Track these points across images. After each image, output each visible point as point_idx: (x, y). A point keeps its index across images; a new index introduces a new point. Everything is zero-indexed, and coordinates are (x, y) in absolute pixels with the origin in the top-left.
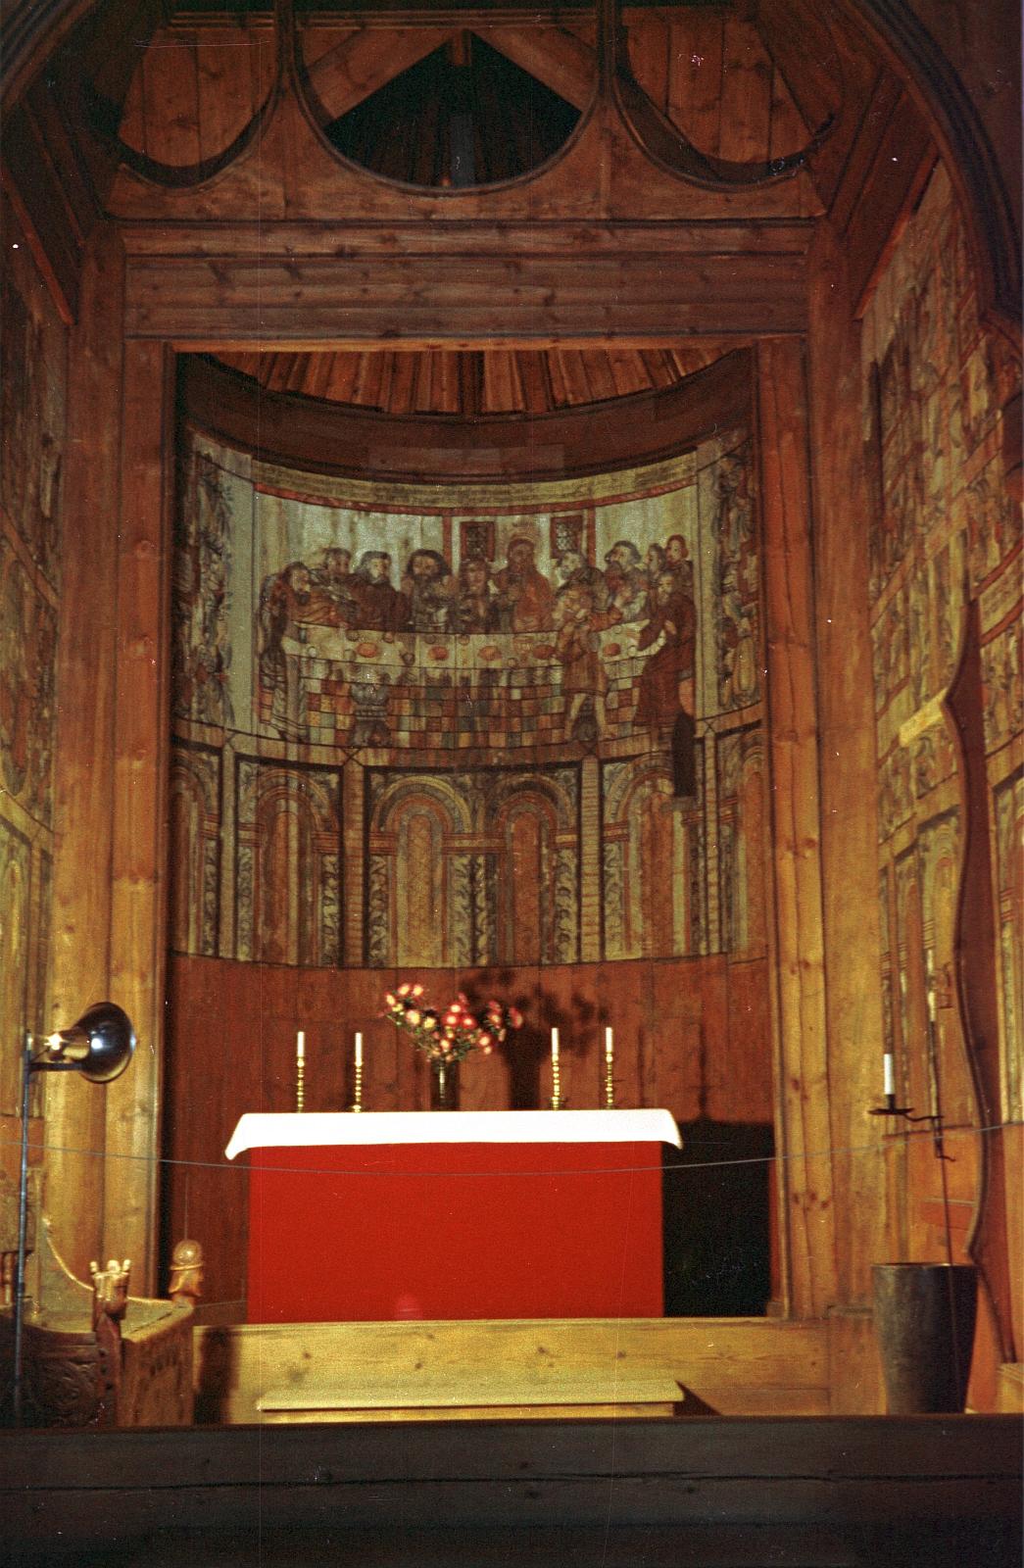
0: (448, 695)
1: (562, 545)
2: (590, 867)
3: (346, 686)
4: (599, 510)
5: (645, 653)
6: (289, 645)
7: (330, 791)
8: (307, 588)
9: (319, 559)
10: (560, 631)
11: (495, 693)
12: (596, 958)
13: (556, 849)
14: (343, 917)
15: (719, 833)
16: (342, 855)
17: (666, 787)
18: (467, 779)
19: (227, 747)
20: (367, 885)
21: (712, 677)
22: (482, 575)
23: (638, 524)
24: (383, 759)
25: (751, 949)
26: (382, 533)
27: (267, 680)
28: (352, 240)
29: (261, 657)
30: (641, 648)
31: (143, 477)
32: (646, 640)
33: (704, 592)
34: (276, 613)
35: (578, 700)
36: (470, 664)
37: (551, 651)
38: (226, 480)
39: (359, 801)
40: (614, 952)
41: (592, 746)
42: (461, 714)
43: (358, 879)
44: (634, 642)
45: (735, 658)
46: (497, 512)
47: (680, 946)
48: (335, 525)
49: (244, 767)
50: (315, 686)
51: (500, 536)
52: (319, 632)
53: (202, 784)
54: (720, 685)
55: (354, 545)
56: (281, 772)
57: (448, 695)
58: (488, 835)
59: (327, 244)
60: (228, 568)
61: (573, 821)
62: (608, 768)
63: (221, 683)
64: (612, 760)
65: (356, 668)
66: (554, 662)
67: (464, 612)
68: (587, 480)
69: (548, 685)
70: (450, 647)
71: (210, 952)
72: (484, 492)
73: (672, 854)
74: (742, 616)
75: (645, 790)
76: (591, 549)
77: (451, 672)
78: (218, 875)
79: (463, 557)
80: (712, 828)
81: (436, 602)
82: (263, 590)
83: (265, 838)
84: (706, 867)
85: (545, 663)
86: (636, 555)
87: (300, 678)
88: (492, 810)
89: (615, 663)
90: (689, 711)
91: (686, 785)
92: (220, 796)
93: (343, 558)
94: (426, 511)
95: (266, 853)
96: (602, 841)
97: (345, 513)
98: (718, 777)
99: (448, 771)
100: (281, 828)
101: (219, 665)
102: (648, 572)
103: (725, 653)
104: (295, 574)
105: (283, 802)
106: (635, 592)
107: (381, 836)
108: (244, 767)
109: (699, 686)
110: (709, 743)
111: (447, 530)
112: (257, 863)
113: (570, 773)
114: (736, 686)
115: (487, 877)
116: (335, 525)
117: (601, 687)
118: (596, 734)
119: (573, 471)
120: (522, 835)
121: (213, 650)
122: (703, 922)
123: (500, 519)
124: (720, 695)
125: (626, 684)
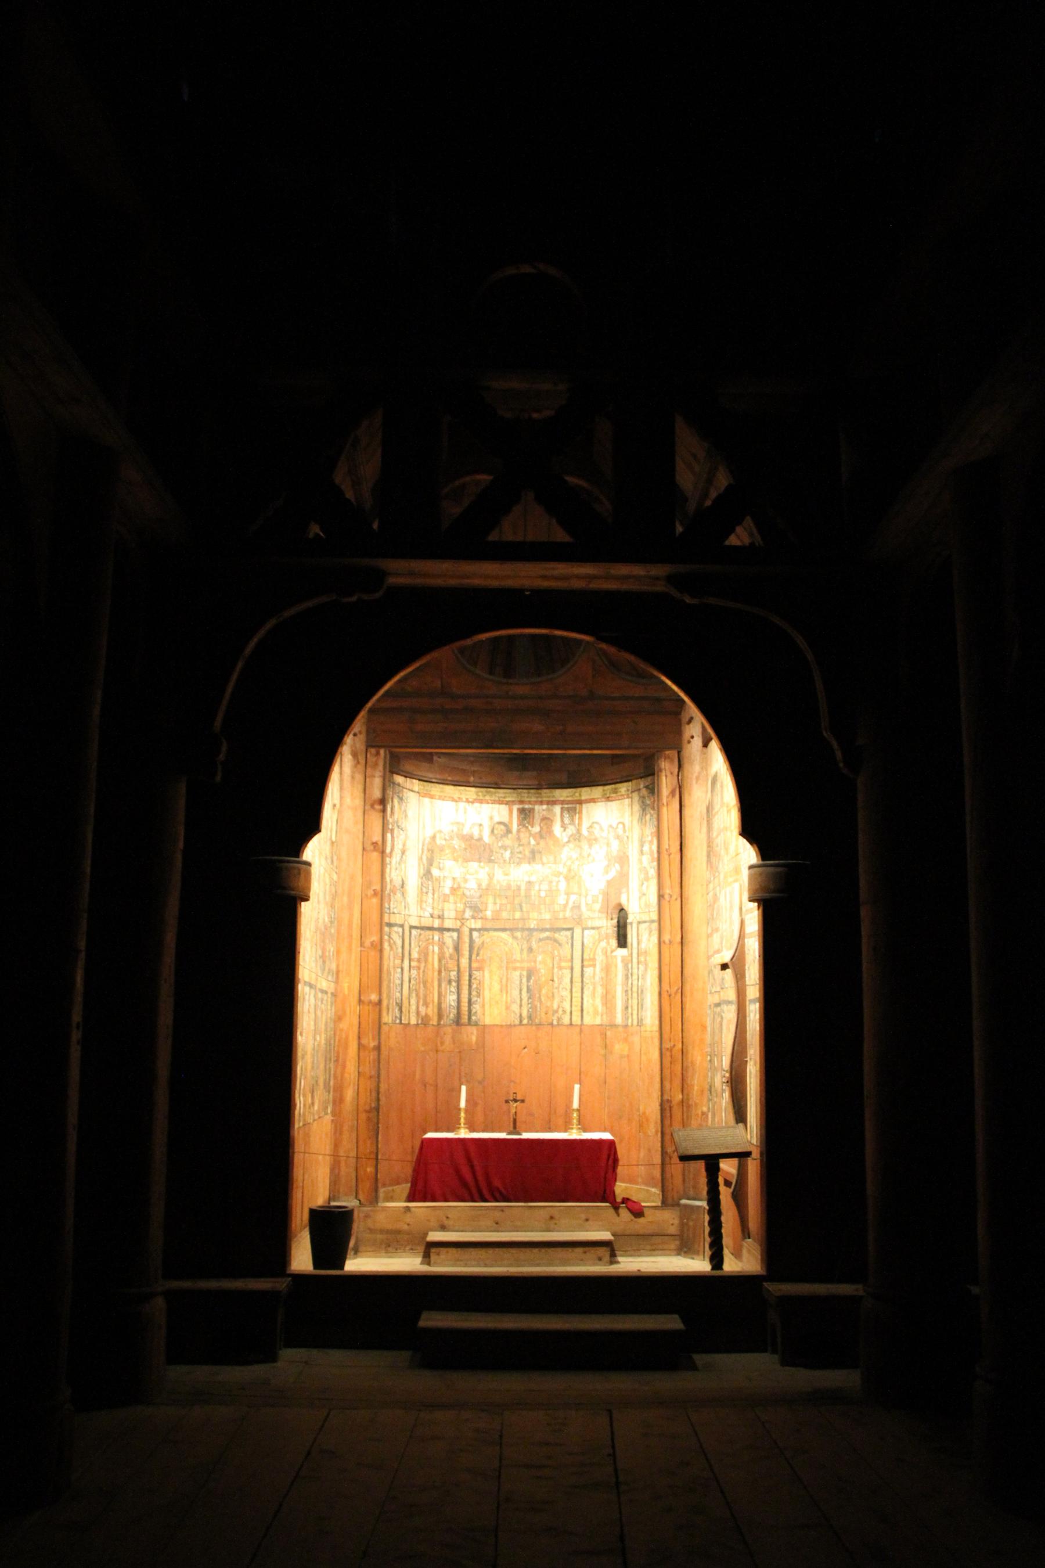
1: (567, 820)
4: (584, 806)
6: (435, 872)
8: (444, 842)
10: (565, 864)
11: (533, 893)
12: (579, 1023)
13: (560, 968)
14: (459, 1001)
16: (459, 971)
17: (614, 942)
18: (518, 934)
20: (470, 986)
22: (527, 835)
24: (478, 924)
25: (653, 1025)
27: (424, 890)
34: (429, 855)
35: (573, 898)
37: (559, 874)
40: (588, 1020)
41: (579, 921)
42: (516, 902)
46: (536, 803)
50: (447, 891)
54: (640, 898)
56: (430, 933)
57: (510, 893)
60: (406, 837)
61: (569, 957)
62: (586, 932)
64: (587, 928)
65: (466, 881)
66: (561, 878)
68: (579, 790)
69: (558, 890)
75: (603, 944)
76: (580, 824)
83: (423, 965)
85: (556, 879)
86: (601, 829)
88: (530, 950)
91: (622, 941)
92: (403, 947)
94: (501, 803)
96: (583, 966)
97: (462, 805)
99: (511, 930)
100: (430, 959)
104: (438, 836)
107: (477, 961)
108: (414, 932)
110: (635, 925)
113: (569, 933)
115: (528, 980)
123: (537, 807)
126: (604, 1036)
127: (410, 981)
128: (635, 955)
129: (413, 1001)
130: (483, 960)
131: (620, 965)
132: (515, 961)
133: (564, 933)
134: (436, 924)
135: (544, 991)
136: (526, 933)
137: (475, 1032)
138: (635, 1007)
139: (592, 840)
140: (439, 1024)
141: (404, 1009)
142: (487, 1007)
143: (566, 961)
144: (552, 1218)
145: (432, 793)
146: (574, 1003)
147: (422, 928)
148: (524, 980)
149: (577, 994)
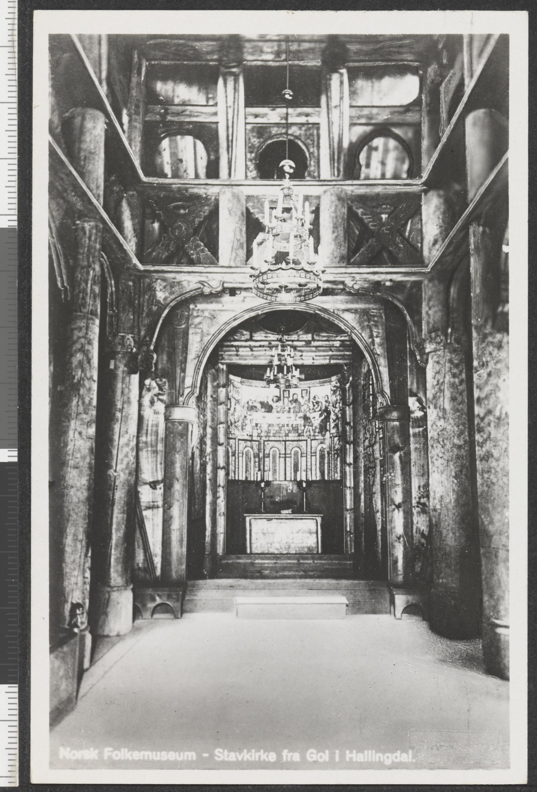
28: (262, 343)
32: (321, 415)
35: (307, 427)
50: (254, 425)
59: (258, 344)
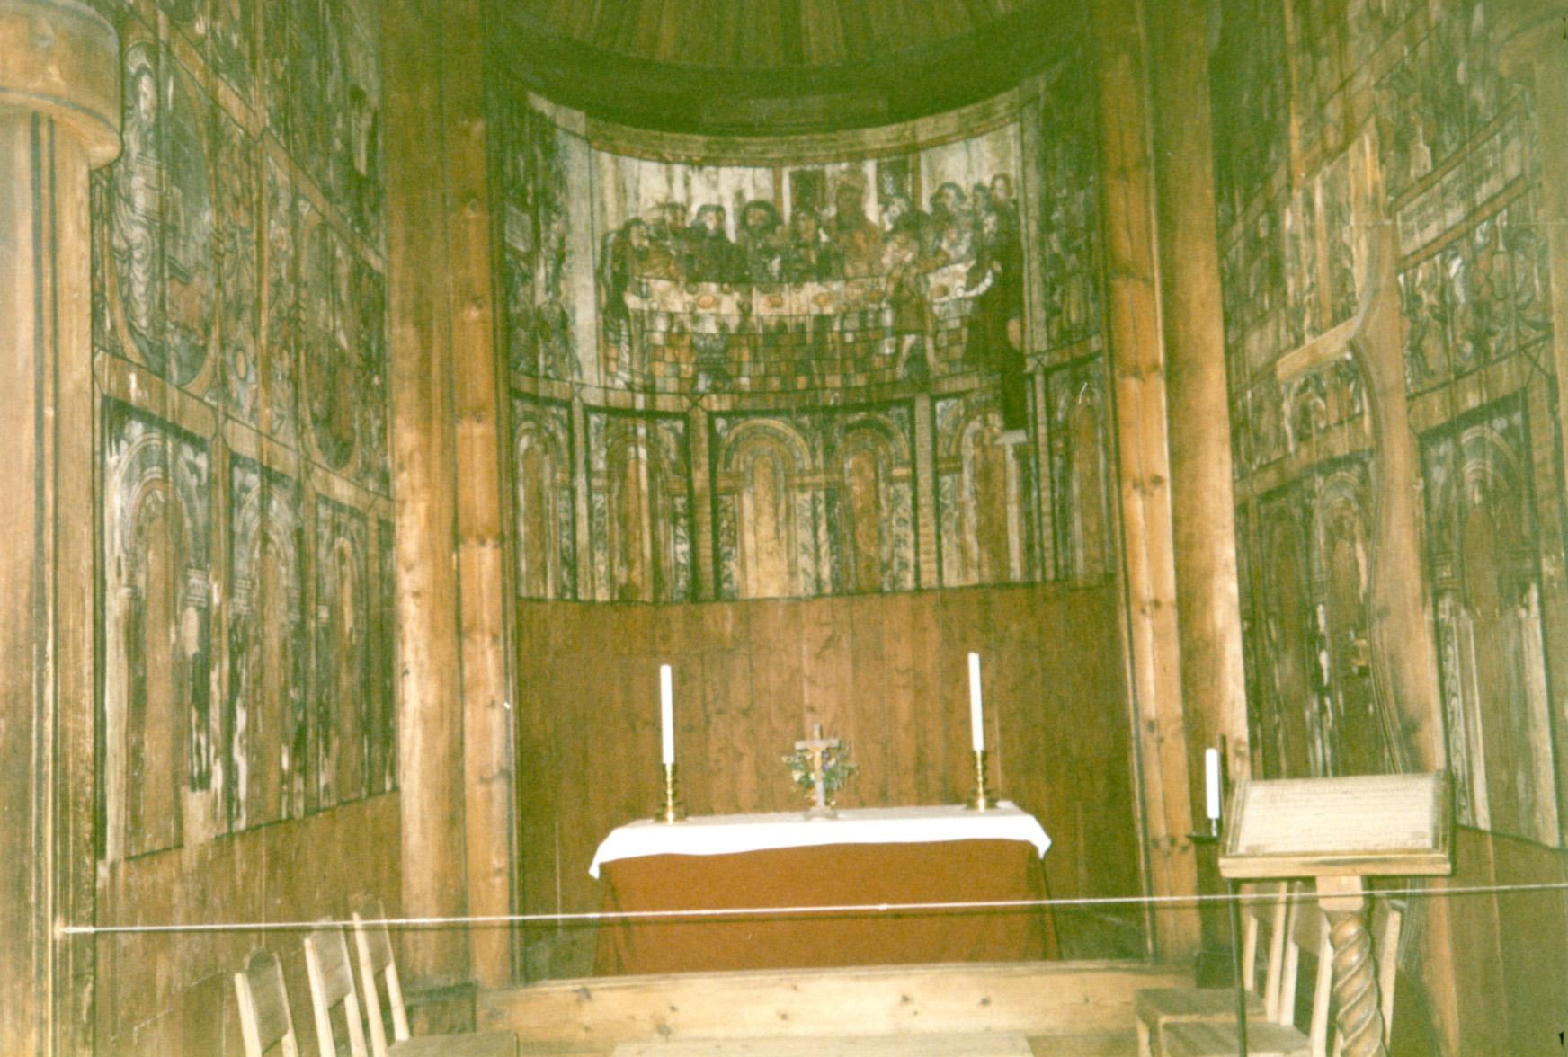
0: (784, 340)
1: (889, 190)
2: (926, 500)
3: (687, 338)
4: (923, 156)
5: (973, 293)
6: (632, 301)
7: (677, 435)
8: (646, 243)
9: (656, 214)
12: (934, 583)
13: (891, 481)
14: (694, 552)
15: (1051, 465)
17: (996, 421)
18: (805, 420)
19: (576, 400)
21: (1040, 315)
22: (812, 223)
23: (963, 165)
24: (726, 405)
26: (715, 185)
27: (611, 336)
29: (605, 312)
30: (967, 289)
31: (467, 132)
32: (973, 278)
33: (1029, 228)
34: (617, 269)
35: (909, 340)
36: (805, 309)
38: (561, 139)
39: (705, 445)
40: (952, 579)
43: (710, 518)
44: (961, 282)
45: (1062, 295)
47: (1016, 570)
48: (670, 180)
49: (594, 419)
50: (658, 338)
51: (830, 186)
52: (661, 285)
53: (553, 437)
54: (1048, 322)
55: (689, 200)
56: (630, 421)
58: (827, 471)
61: (907, 456)
62: (940, 405)
63: (567, 342)
64: (945, 397)
65: (696, 319)
66: (884, 305)
67: (796, 261)
68: (910, 124)
69: (879, 327)
70: (785, 296)
71: (568, 596)
72: (811, 141)
73: (1005, 484)
74: (1069, 251)
75: (975, 425)
77: (787, 321)
78: (573, 523)
79: (794, 207)
80: (1044, 458)
81: (770, 252)
82: (604, 247)
83: (617, 485)
84: (1039, 497)
86: (961, 196)
87: (643, 331)
88: (830, 449)
89: (943, 304)
90: (1017, 346)
93: (679, 213)
94: (755, 164)
95: (619, 497)
96: (937, 474)
97: (678, 170)
98: (1050, 410)
99: (788, 412)
100: (631, 472)
101: (564, 322)
102: (974, 213)
103: (1053, 290)
104: (634, 230)
105: (632, 450)
106: (960, 234)
107: (729, 476)
108: (594, 419)
109: (1028, 321)
110: (1039, 379)
111: (777, 182)
112: (611, 510)
113: (904, 411)
114: (1065, 324)
116: (670, 180)
117: (930, 327)
118: (927, 372)
119: (898, 114)
120: (859, 470)
121: (557, 309)
122: (1037, 549)
123: (830, 169)
124: (1048, 331)
125: (954, 324)
126: (986, 604)
127: (590, 516)
128: (1042, 438)
129: (599, 557)
130: (739, 476)
131: (1013, 466)
132: (802, 472)
133: (895, 411)
134: (640, 402)
135: (861, 528)
136: (819, 417)
137: (730, 613)
138: (1048, 544)
139: (943, 218)
140: (656, 602)
141: (580, 570)
142: (750, 564)
143: (903, 465)
144: (906, 999)
145: (617, 143)
146: (922, 548)
147: (611, 411)
148: (821, 508)
149: (928, 530)
